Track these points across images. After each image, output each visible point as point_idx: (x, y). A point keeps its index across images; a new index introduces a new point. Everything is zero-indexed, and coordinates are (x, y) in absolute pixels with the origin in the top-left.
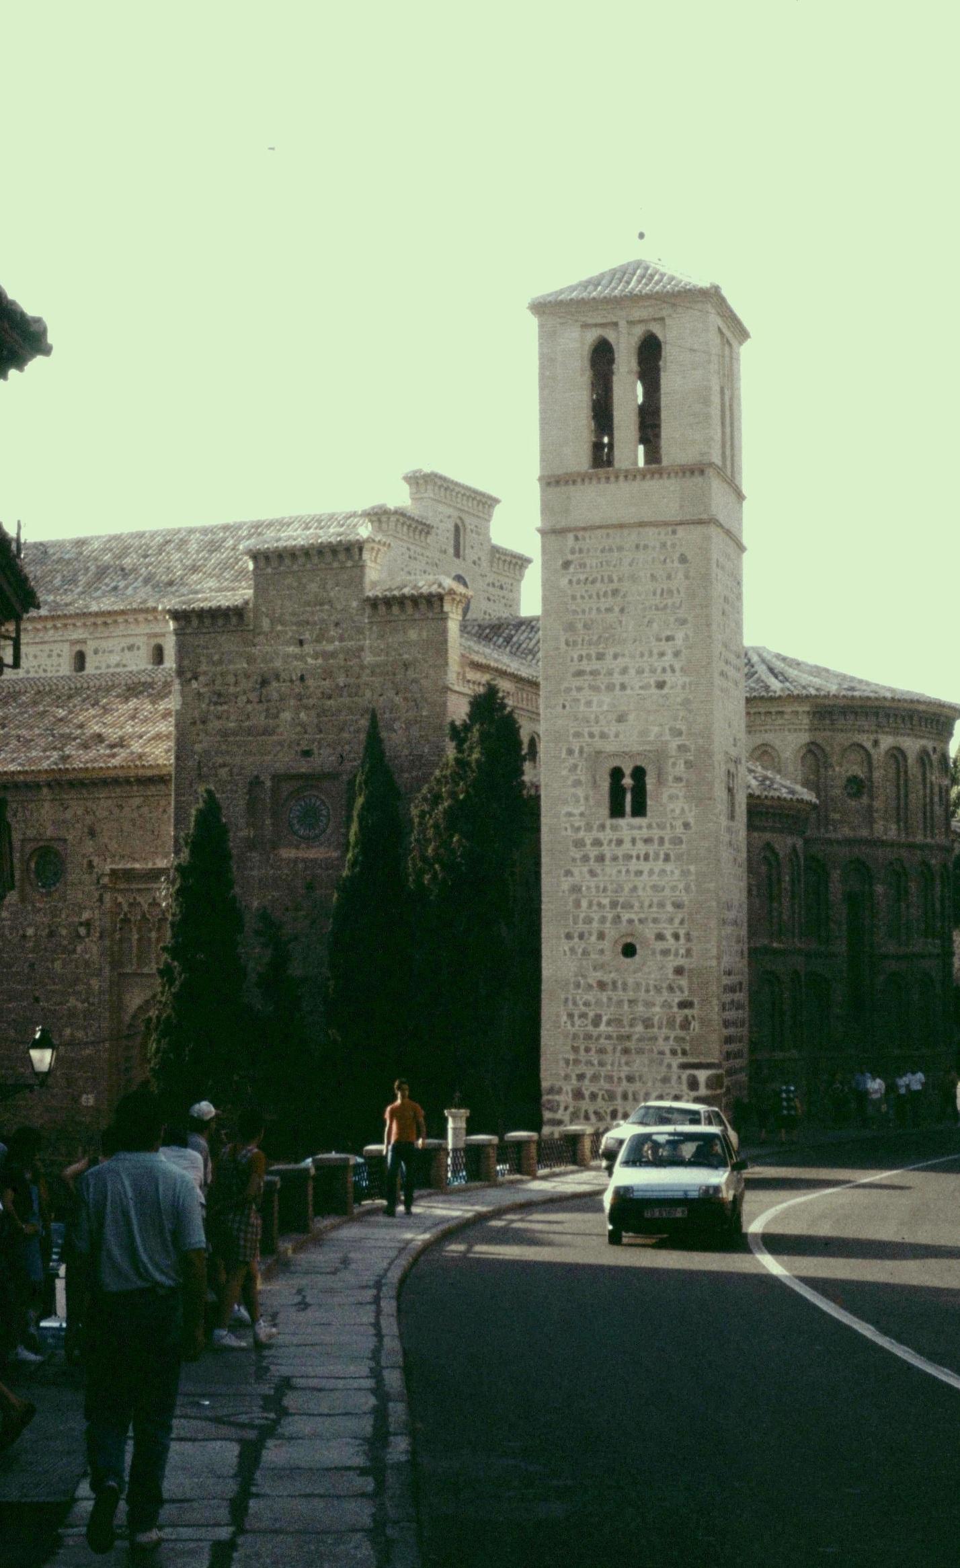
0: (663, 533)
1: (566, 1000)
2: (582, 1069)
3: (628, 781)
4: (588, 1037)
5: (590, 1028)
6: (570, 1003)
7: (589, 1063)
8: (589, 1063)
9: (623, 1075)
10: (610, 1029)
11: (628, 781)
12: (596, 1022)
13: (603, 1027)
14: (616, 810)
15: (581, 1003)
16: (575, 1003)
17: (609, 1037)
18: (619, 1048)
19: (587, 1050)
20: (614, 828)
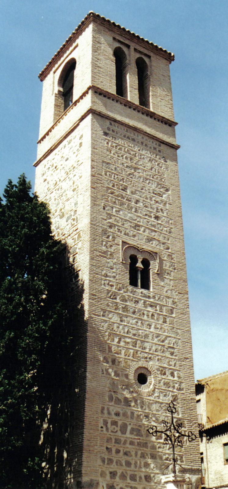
0: (154, 143)
1: (103, 409)
2: (114, 467)
3: (139, 265)
4: (117, 441)
5: (119, 433)
6: (106, 412)
7: (119, 463)
8: (119, 463)
9: (143, 475)
10: (133, 436)
11: (139, 265)
12: (123, 431)
13: (128, 435)
14: (133, 283)
15: (113, 413)
16: (109, 413)
17: (132, 443)
18: (139, 453)
19: (118, 451)
20: (133, 292)
